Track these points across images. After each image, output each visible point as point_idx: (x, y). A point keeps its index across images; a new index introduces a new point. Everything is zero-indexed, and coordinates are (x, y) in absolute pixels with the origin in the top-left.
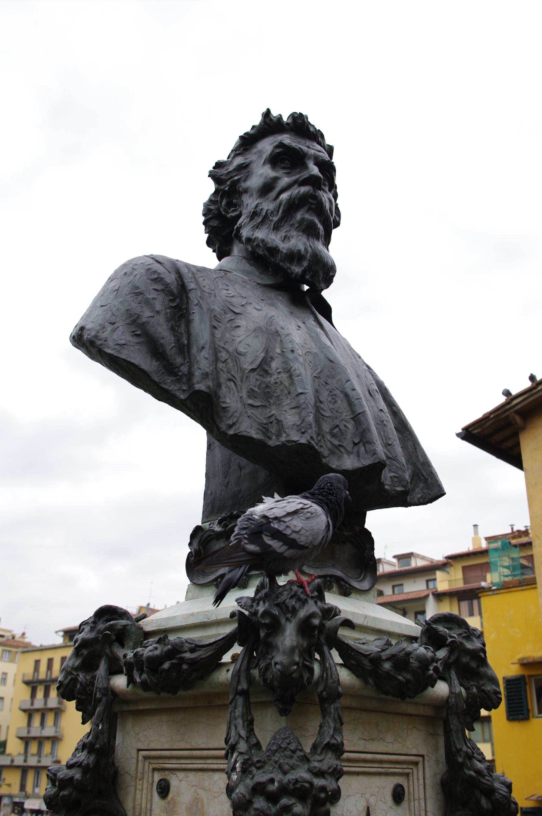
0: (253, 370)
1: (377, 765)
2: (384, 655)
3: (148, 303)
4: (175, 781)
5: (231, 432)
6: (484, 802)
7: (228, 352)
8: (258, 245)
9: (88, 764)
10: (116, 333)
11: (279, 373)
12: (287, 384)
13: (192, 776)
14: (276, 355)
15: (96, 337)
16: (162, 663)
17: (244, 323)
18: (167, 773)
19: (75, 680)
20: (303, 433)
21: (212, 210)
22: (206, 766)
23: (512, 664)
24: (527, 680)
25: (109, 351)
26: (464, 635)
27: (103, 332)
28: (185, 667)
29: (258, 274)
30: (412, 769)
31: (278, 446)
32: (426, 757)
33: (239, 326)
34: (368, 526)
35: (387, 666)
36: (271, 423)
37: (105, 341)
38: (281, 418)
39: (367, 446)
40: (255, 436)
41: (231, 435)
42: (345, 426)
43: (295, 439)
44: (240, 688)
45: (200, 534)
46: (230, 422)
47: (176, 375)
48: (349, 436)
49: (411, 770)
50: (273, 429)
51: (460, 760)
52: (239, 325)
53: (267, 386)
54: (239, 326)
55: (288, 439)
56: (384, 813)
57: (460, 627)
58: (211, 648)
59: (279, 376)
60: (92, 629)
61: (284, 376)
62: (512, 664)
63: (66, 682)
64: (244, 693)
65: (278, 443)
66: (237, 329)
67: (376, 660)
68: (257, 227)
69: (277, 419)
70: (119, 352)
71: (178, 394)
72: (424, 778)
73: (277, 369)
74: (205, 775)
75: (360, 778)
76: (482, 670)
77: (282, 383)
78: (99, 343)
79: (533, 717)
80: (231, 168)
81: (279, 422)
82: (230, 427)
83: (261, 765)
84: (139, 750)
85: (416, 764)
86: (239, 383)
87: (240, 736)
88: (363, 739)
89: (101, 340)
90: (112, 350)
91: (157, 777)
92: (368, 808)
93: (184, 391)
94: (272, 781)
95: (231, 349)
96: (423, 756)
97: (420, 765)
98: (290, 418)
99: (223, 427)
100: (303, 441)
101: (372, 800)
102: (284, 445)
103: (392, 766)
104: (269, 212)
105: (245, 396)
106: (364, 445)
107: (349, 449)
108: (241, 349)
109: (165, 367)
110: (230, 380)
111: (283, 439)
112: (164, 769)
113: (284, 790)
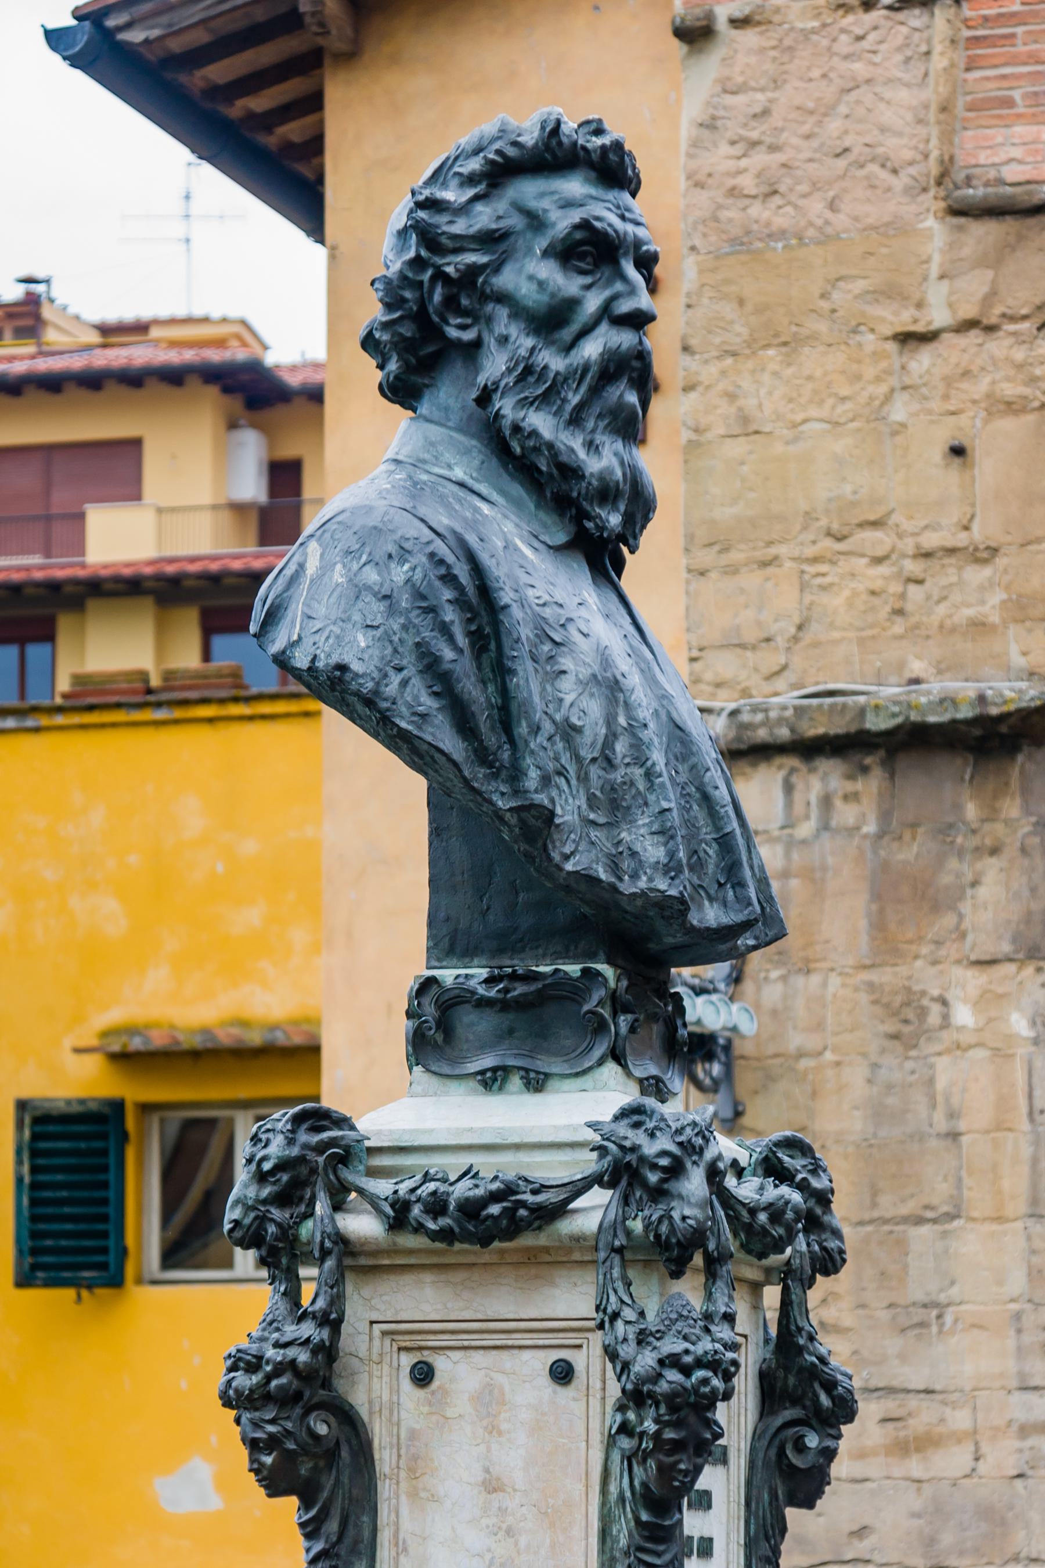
0: (594, 760)
3: (445, 630)
4: (441, 1363)
5: (569, 867)
7: (554, 722)
8: (536, 450)
9: (322, 1340)
10: (408, 689)
11: (628, 765)
12: (641, 788)
13: (478, 1356)
14: (619, 730)
15: (376, 692)
16: (485, 1206)
17: (572, 667)
18: (426, 1353)
19: (263, 1219)
20: (672, 878)
21: (404, 300)
22: (510, 1343)
23: (78, 1051)
24: (131, 1123)
25: (403, 725)
26: (810, 1167)
27: (387, 685)
28: (522, 1212)
29: (532, 506)
31: (634, 894)
33: (564, 672)
35: (763, 1217)
36: (621, 853)
37: (394, 703)
38: (638, 848)
39: (738, 889)
40: (603, 876)
41: (569, 873)
42: (705, 852)
43: (662, 886)
44: (617, 1243)
45: (434, 990)
46: (567, 850)
47: (491, 767)
48: (711, 868)
50: (626, 864)
51: (801, 1342)
52: (564, 668)
53: (613, 789)
54: (564, 672)
55: (652, 885)
57: (804, 1154)
58: (564, 1189)
59: (628, 771)
60: (291, 1142)
61: (638, 772)
62: (78, 1051)
63: (247, 1221)
64: (620, 1251)
65: (634, 890)
66: (563, 676)
68: (532, 404)
69: (630, 849)
70: (420, 728)
71: (495, 798)
73: (624, 757)
74: (505, 1355)
76: (826, 1218)
77: (632, 784)
78: (384, 705)
79: (139, 1281)
80: (460, 227)
81: (634, 854)
82: (567, 857)
83: (659, 1335)
84: (372, 1323)
86: (574, 782)
87: (622, 1302)
89: (386, 699)
90: (408, 723)
91: (407, 1361)
93: (503, 794)
94: (687, 1352)
95: (558, 717)
98: (653, 852)
99: (556, 856)
100: (673, 892)
102: (643, 894)
104: (560, 378)
105: (584, 806)
106: (733, 887)
107: (712, 892)
108: (574, 720)
109: (475, 751)
110: (559, 774)
111: (643, 883)
112: (420, 1349)
113: (699, 1363)
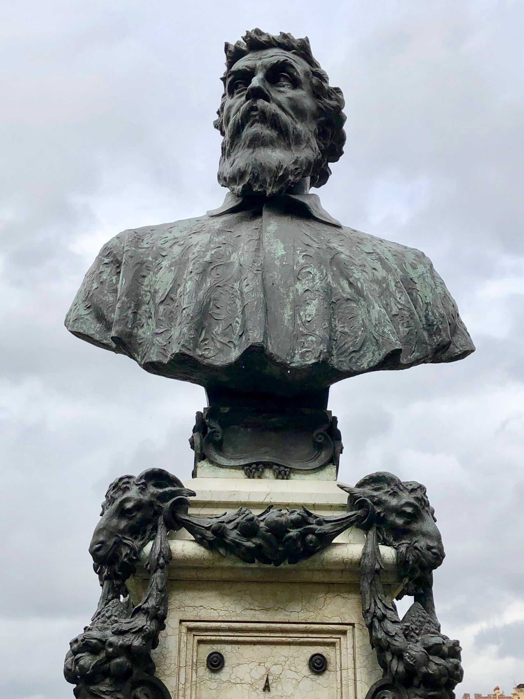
1: (280, 635)
6: (396, 666)
30: (340, 638)
32: (356, 625)
35: (233, 535)
49: (338, 640)
56: (294, 682)
67: (219, 532)
72: (354, 647)
75: (258, 647)
85: (344, 633)
88: (252, 609)
92: (268, 675)
96: (353, 625)
97: (349, 635)
101: (275, 670)
103: (305, 635)
108: (157, 288)
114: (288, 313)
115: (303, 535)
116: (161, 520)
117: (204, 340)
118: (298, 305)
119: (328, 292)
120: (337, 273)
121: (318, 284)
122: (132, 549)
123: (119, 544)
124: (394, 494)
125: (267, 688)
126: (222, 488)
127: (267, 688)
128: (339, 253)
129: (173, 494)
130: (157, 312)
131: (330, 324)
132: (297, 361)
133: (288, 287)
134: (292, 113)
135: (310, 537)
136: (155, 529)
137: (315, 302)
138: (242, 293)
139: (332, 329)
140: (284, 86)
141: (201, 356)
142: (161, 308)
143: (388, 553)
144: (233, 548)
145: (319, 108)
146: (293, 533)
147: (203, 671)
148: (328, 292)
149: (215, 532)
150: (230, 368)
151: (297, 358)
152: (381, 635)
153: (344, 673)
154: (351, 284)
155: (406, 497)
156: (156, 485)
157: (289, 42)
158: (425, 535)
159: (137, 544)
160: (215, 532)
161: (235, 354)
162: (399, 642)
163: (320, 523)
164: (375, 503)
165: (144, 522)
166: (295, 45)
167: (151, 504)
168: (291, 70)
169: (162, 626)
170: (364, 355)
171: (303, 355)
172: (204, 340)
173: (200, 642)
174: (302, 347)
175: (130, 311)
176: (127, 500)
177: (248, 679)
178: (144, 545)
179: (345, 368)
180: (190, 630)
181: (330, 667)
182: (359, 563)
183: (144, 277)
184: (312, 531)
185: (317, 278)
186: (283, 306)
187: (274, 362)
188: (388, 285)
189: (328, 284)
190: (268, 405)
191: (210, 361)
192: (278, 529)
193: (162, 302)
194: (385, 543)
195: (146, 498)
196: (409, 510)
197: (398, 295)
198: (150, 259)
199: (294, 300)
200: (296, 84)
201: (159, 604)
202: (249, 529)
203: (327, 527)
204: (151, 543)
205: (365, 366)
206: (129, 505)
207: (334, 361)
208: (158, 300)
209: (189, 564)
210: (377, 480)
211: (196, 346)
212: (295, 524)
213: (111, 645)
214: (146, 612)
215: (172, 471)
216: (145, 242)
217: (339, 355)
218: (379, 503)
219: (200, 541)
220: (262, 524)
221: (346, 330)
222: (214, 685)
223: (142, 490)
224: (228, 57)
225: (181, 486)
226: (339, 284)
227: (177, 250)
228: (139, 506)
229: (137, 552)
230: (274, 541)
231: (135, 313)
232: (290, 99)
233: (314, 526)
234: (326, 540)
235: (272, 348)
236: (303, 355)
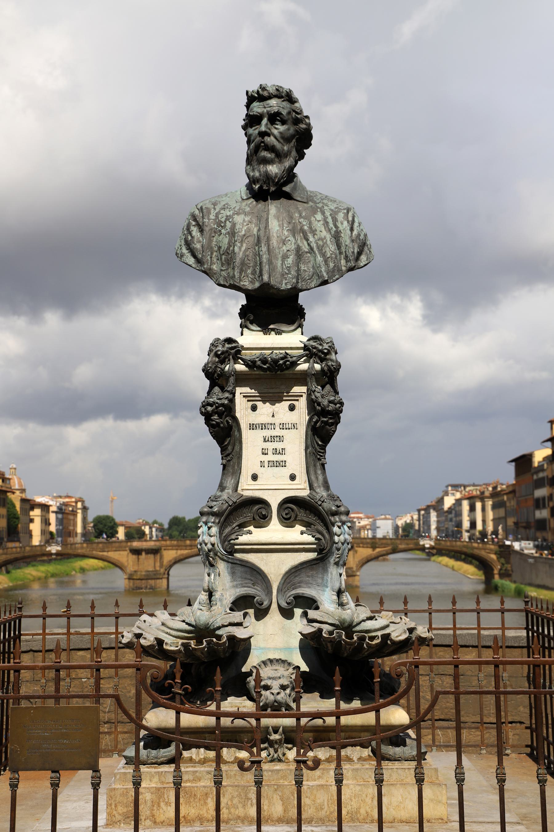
2: (257, 360)
6: (319, 408)
34: (300, 301)
35: (259, 363)
67: (254, 362)
114: (279, 263)
115: (285, 363)
116: (231, 357)
117: (244, 277)
118: (285, 257)
119: (298, 249)
120: (302, 237)
121: (293, 247)
122: (221, 369)
123: (216, 367)
124: (321, 345)
125: (273, 416)
126: (254, 340)
127: (273, 416)
128: (303, 225)
129: (235, 347)
130: (221, 259)
131: (298, 268)
132: (283, 287)
133: (279, 248)
134: (282, 141)
135: (288, 363)
136: (229, 360)
137: (291, 257)
138: (259, 253)
139: (299, 270)
140: (277, 125)
141: (243, 285)
142: (223, 257)
143: (318, 367)
144: (260, 368)
145: (296, 131)
146: (281, 362)
147: (250, 410)
148: (298, 249)
149: (252, 362)
150: (255, 290)
151: (284, 284)
152: (313, 397)
153: (302, 410)
154: (309, 244)
155: (326, 346)
156: (228, 344)
157: (280, 94)
158: (332, 360)
159: (223, 366)
160: (252, 362)
161: (257, 285)
162: (320, 400)
163: (291, 358)
164: (313, 348)
165: (225, 358)
166: (283, 95)
167: (227, 351)
168: (281, 116)
169: (234, 396)
170: (313, 281)
171: (285, 286)
172: (244, 277)
173: (248, 401)
174: (286, 280)
175: (209, 257)
176: (218, 351)
177: (266, 413)
178: (225, 367)
179: (304, 288)
180: (244, 396)
181: (296, 408)
182: (307, 371)
183: (213, 237)
184: (288, 361)
185: (293, 243)
186: (277, 259)
187: (274, 288)
188: (326, 241)
189: (298, 246)
190: (271, 306)
191: (247, 287)
192: (275, 361)
193: (223, 254)
194: (317, 363)
195: (225, 349)
196: (326, 351)
197: (331, 246)
198: (215, 226)
199: (283, 256)
200: (283, 122)
201: (233, 388)
202: (264, 361)
203: (294, 359)
204: (228, 366)
205: (313, 286)
206: (219, 353)
207: (300, 286)
208: (221, 253)
209: (241, 373)
210: (315, 338)
211: (240, 280)
212: (282, 359)
213: (217, 403)
214: (228, 391)
215: (234, 337)
216: (212, 214)
217: (302, 282)
218: (315, 348)
219: (247, 365)
220: (269, 359)
221: (306, 269)
222: (254, 415)
223: (223, 346)
224: (248, 99)
225: (238, 343)
226: (303, 243)
227: (228, 225)
228: (223, 353)
229: (223, 370)
230: (274, 365)
231: (211, 257)
232: (281, 133)
233: (289, 359)
234: (294, 364)
235: (273, 282)
236: (286, 284)
